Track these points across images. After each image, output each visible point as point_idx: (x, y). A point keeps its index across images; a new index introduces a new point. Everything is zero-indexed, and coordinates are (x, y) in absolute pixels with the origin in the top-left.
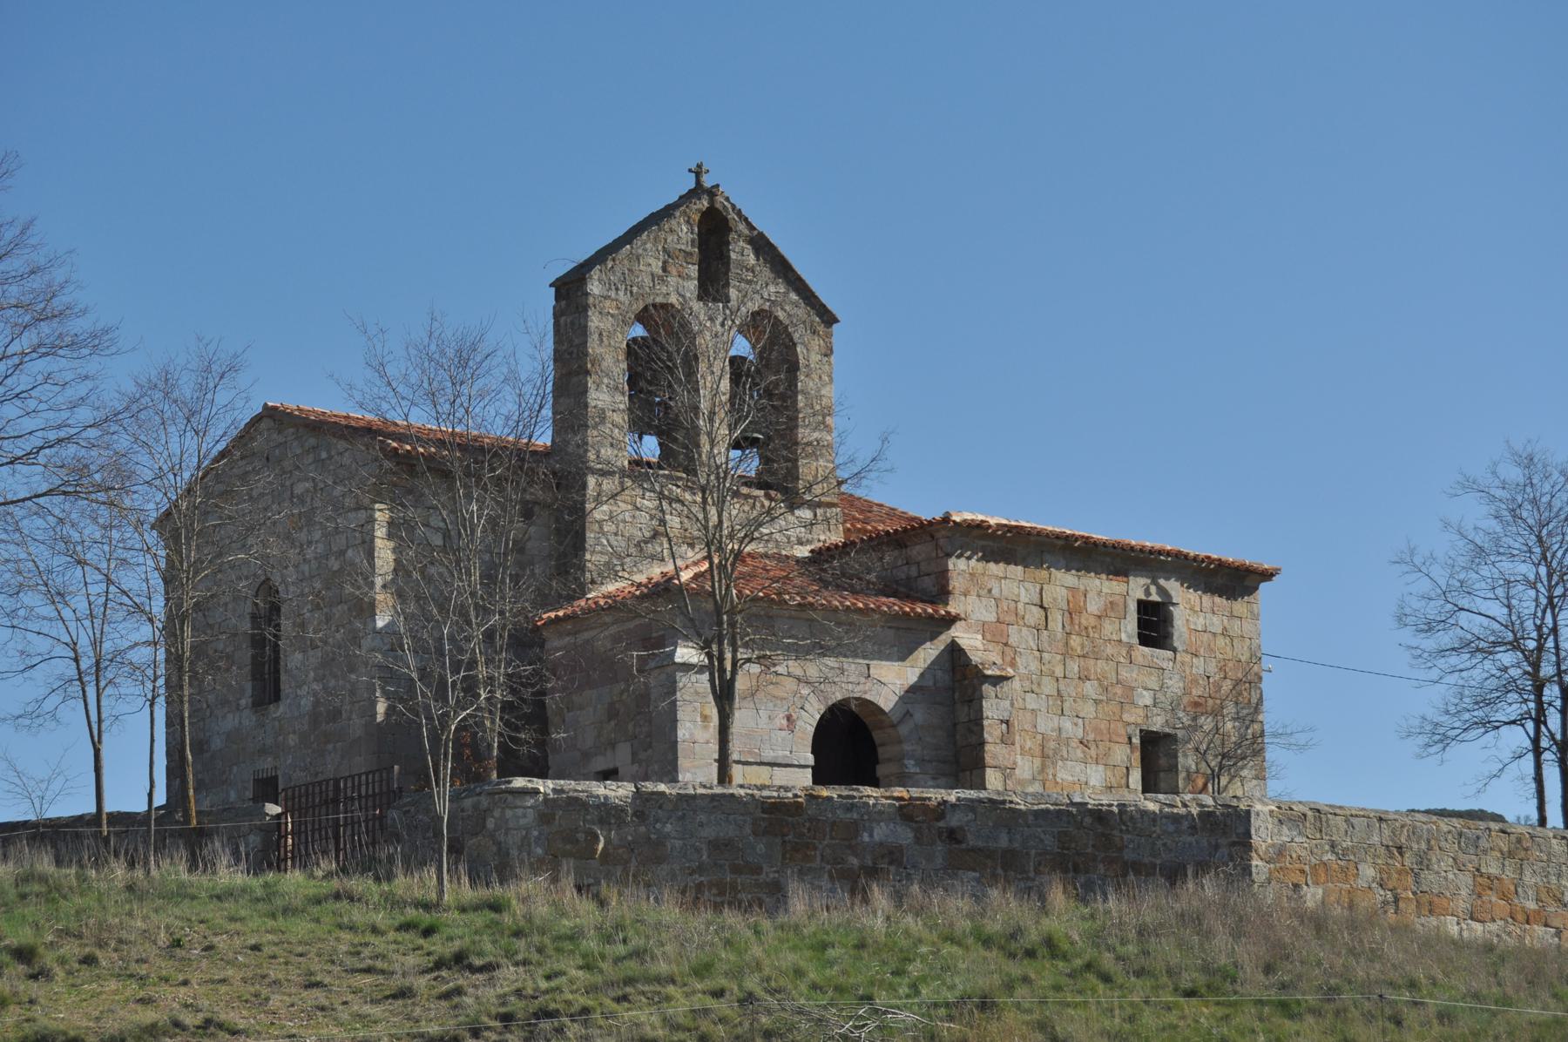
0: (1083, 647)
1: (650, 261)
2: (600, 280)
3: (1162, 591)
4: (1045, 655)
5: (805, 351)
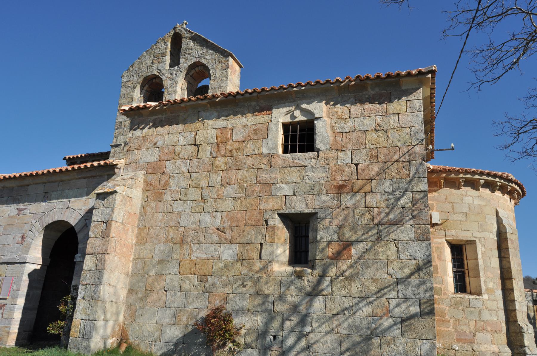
0: (226, 164)
1: (147, 62)
2: (127, 76)
3: (305, 112)
4: (194, 175)
5: (214, 71)
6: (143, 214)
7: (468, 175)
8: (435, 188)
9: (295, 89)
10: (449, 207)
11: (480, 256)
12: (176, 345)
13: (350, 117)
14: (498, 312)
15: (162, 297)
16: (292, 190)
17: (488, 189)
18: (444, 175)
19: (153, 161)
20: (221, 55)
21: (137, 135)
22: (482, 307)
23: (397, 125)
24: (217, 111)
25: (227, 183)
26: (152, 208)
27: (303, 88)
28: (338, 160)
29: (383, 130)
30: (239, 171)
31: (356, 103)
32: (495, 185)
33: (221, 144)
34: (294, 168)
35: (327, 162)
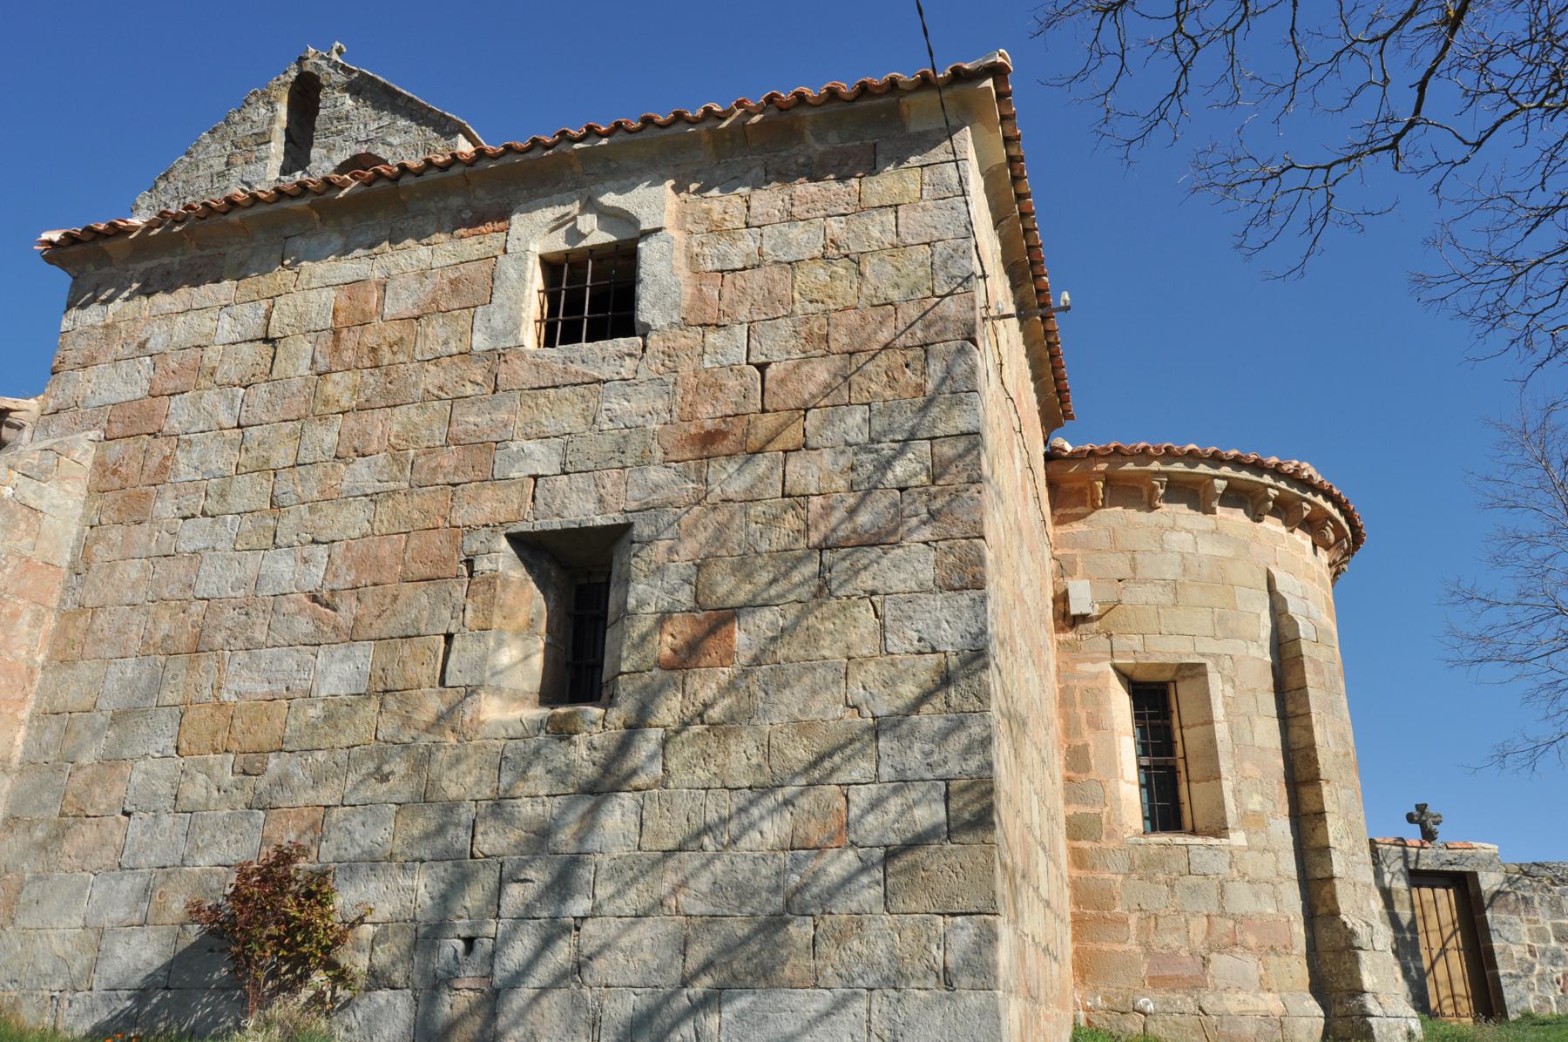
0: (356, 390)
1: (212, 162)
3: (611, 217)
6: (81, 569)
7: (1177, 464)
8: (1080, 510)
9: (577, 146)
10: (1121, 566)
11: (1219, 712)
12: (142, 994)
13: (748, 226)
14: (1281, 887)
15: (111, 833)
16: (556, 459)
17: (1242, 511)
18: (1103, 467)
19: (130, 397)
20: (434, 131)
21: (89, 321)
22: (1228, 871)
23: (890, 238)
24: (342, 233)
25: (356, 451)
26: (111, 548)
27: (604, 141)
28: (706, 356)
29: (847, 256)
30: (396, 410)
31: (768, 183)
32: (1262, 496)
33: (345, 330)
34: (567, 389)
35: (671, 365)
